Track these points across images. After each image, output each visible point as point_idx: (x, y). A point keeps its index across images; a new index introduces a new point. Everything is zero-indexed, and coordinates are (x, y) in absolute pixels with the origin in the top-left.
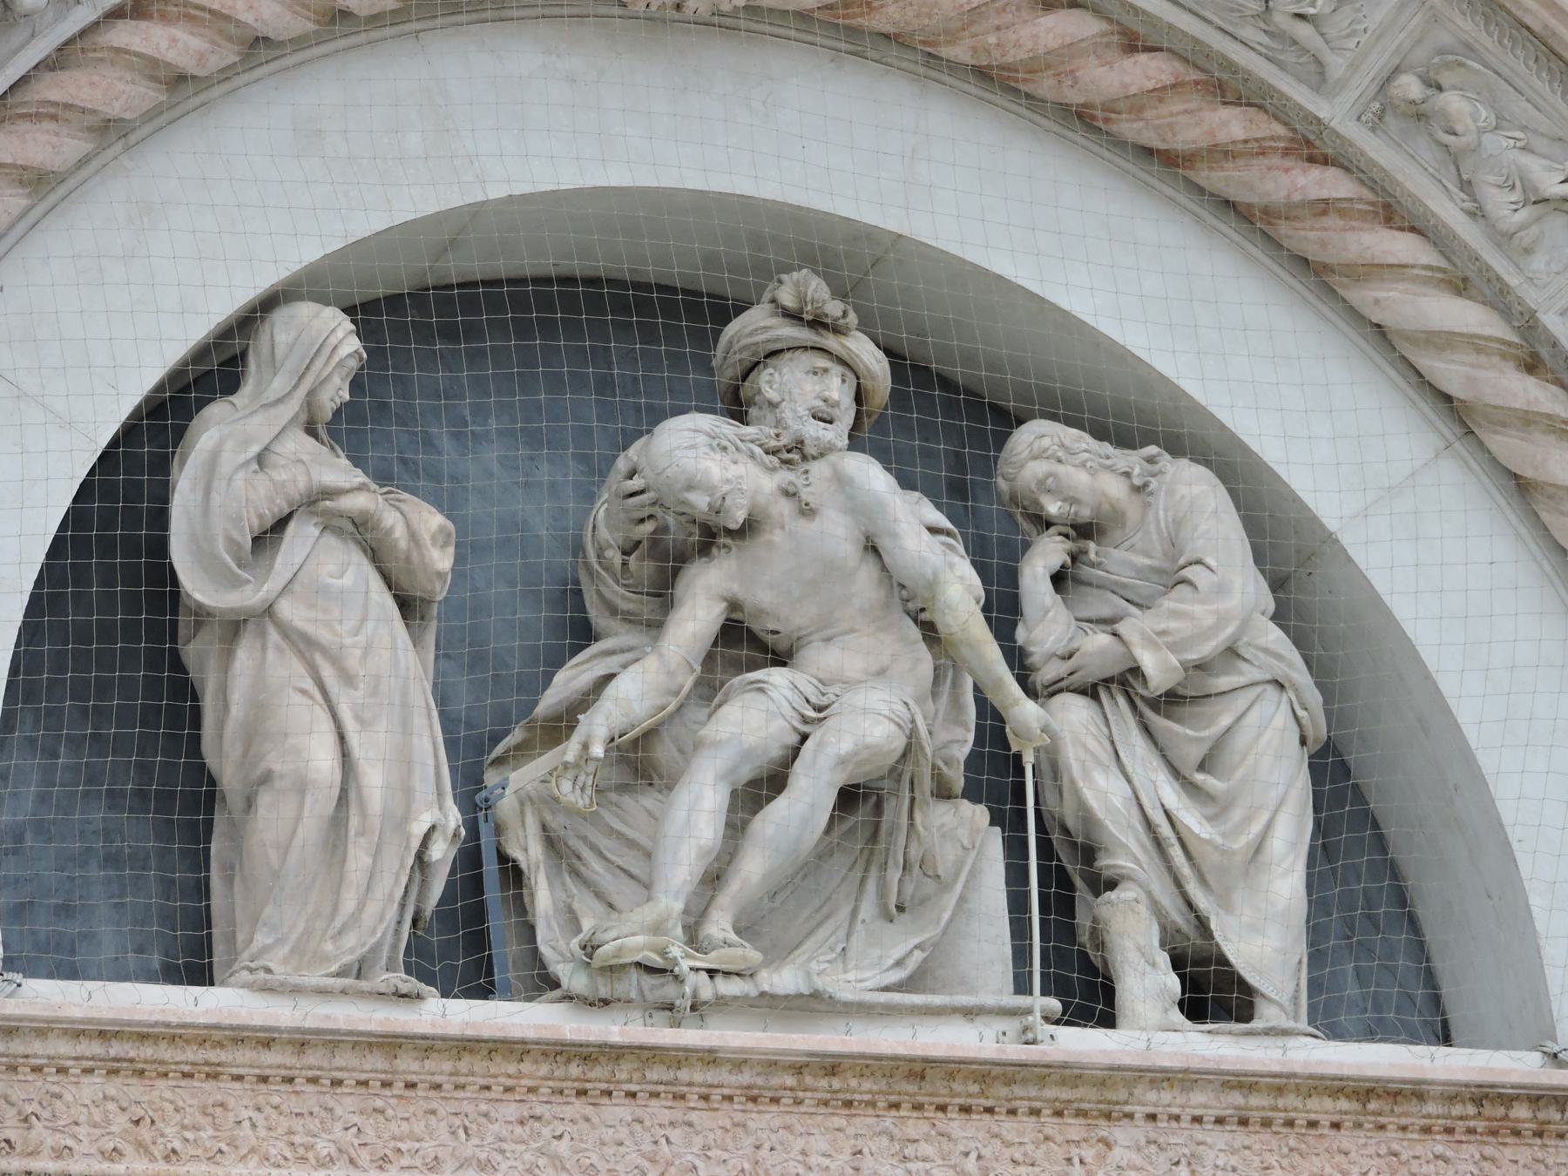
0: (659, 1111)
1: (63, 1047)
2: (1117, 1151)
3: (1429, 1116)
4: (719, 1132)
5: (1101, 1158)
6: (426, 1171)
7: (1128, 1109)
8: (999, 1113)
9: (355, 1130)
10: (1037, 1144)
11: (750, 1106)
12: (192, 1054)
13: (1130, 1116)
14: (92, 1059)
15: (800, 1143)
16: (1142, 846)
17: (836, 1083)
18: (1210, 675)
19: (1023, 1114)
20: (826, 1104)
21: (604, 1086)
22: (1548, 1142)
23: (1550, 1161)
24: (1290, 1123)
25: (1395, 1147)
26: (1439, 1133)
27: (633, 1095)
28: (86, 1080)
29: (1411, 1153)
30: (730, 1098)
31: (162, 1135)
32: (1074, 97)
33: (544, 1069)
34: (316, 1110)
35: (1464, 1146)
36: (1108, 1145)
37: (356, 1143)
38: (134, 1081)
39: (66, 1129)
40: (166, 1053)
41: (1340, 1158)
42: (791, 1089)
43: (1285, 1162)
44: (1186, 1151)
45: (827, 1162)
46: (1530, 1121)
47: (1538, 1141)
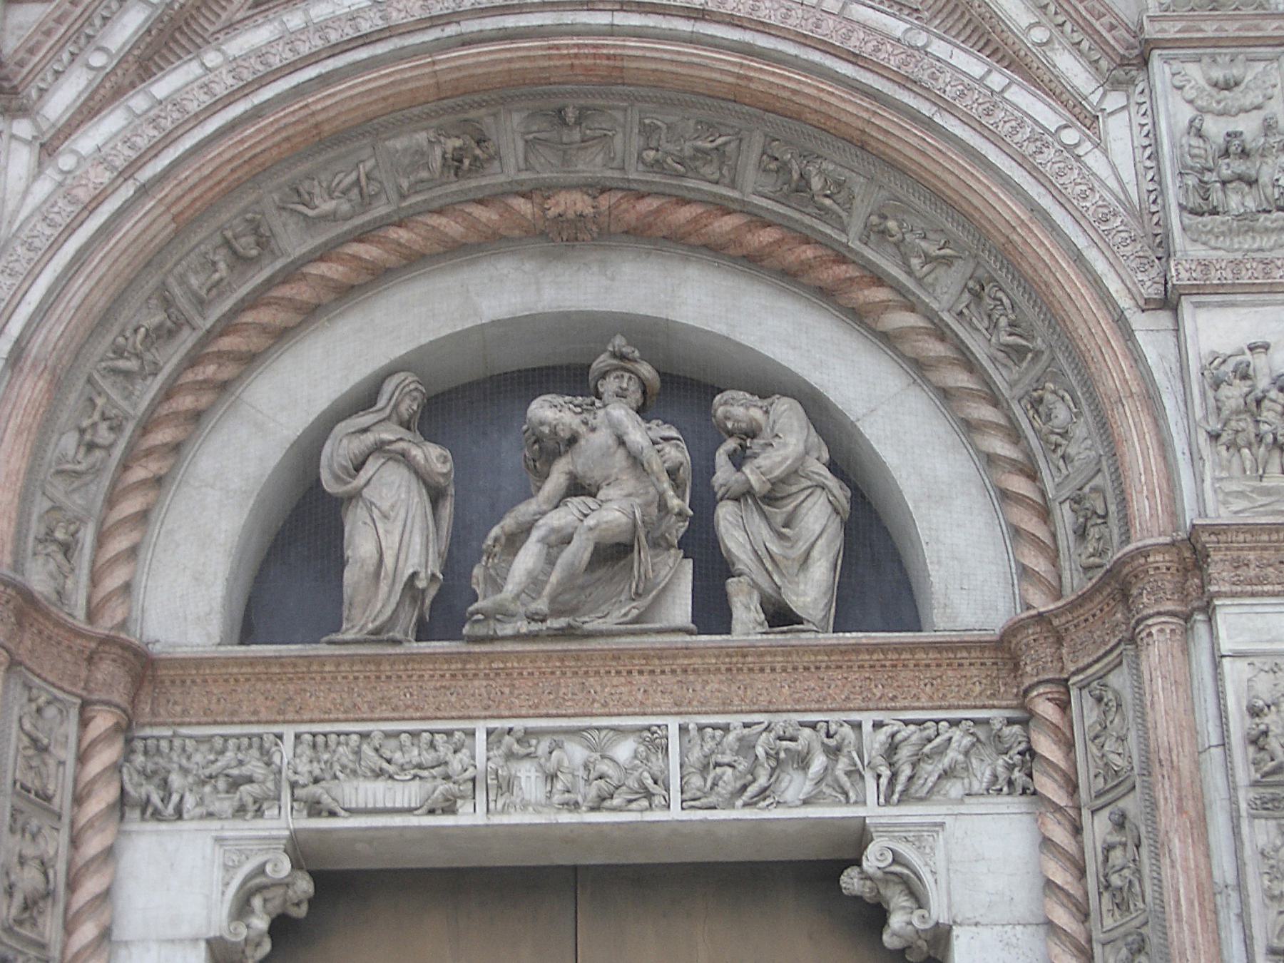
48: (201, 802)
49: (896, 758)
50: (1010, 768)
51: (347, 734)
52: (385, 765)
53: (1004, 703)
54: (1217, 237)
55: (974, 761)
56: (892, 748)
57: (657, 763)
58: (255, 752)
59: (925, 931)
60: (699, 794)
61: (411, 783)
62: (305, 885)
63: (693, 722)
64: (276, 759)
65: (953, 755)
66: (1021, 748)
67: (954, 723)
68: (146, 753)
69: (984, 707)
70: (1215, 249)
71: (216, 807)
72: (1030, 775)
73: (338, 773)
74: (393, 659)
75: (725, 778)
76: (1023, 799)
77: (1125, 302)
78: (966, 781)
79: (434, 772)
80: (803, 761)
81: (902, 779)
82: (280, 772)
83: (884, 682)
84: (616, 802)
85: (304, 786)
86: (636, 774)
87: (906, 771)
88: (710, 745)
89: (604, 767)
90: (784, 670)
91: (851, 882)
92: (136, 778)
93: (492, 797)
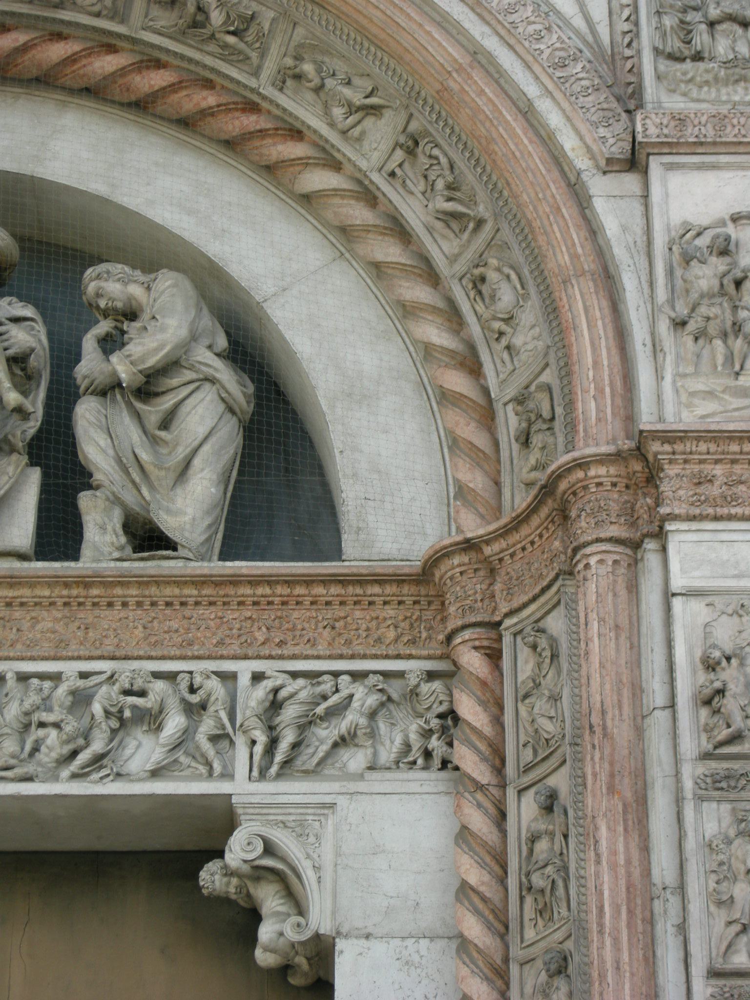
16: (113, 468)
18: (167, 377)
26: (249, 605)
32: (133, 98)
49: (278, 720)
50: (427, 734)
53: (425, 653)
54: (700, 87)
56: (275, 705)
59: (302, 943)
60: (12, 762)
67: (357, 676)
69: (398, 657)
70: (698, 101)
72: (450, 744)
75: (49, 742)
76: (443, 774)
77: (582, 162)
78: (370, 751)
81: (284, 746)
83: (270, 622)
87: (288, 738)
88: (33, 699)
90: (139, 604)
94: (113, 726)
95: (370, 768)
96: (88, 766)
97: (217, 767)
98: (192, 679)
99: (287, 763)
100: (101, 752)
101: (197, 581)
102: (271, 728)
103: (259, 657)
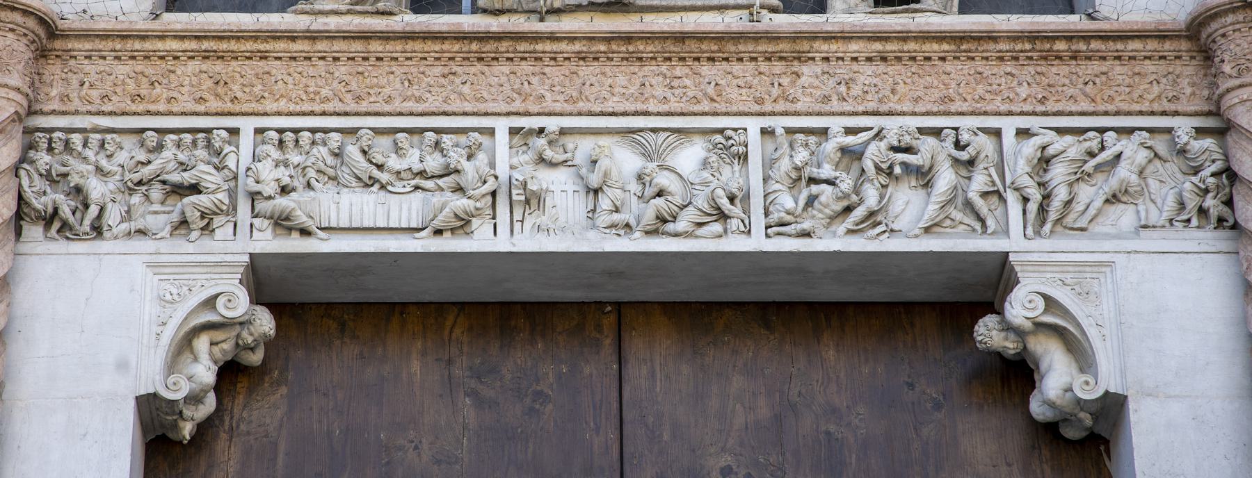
0: (526, 67)
1: (174, 45)
2: (803, 79)
3: (1000, 51)
4: (562, 77)
5: (793, 83)
6: (384, 104)
7: (810, 55)
8: (732, 61)
9: (344, 83)
10: (754, 76)
11: (582, 63)
12: (249, 46)
13: (813, 59)
14: (192, 51)
15: (610, 81)
17: (631, 48)
19: (747, 61)
20: (627, 59)
21: (493, 55)
22: (1080, 62)
23: (1080, 74)
24: (913, 59)
25: (980, 69)
26: (1009, 60)
27: (511, 59)
28: (191, 63)
29: (990, 73)
30: (569, 59)
31: (230, 90)
33: (456, 47)
34: (323, 74)
35: (1026, 67)
36: (798, 76)
37: (343, 90)
38: (219, 62)
39: (176, 89)
40: (233, 45)
41: (944, 77)
42: (605, 53)
43: (909, 81)
44: (846, 77)
45: (624, 91)
46: (1067, 51)
47: (1074, 62)
48: (128, 215)
49: (1048, 177)
51: (326, 131)
52: (376, 173)
55: (1150, 181)
56: (1044, 161)
57: (730, 176)
58: (201, 153)
60: (789, 218)
61: (412, 195)
62: (265, 323)
63: (779, 123)
64: (231, 162)
65: (1124, 172)
66: (1213, 168)
67: (1122, 131)
68: (50, 149)
69: (1164, 113)
71: (151, 222)
72: (1229, 203)
73: (313, 182)
74: (386, 37)
75: (823, 199)
79: (441, 182)
80: (924, 177)
82: (235, 178)
84: (681, 225)
85: (270, 198)
86: (708, 190)
87: (1061, 194)
89: (664, 180)
91: (988, 332)
92: (40, 184)
93: (518, 215)
94: (884, 183)
95: (1145, 227)
96: (862, 222)
97: (991, 223)
98: (957, 135)
99: (1058, 221)
100: (876, 209)
101: (956, 36)
102: (1041, 185)
103: (1022, 114)
